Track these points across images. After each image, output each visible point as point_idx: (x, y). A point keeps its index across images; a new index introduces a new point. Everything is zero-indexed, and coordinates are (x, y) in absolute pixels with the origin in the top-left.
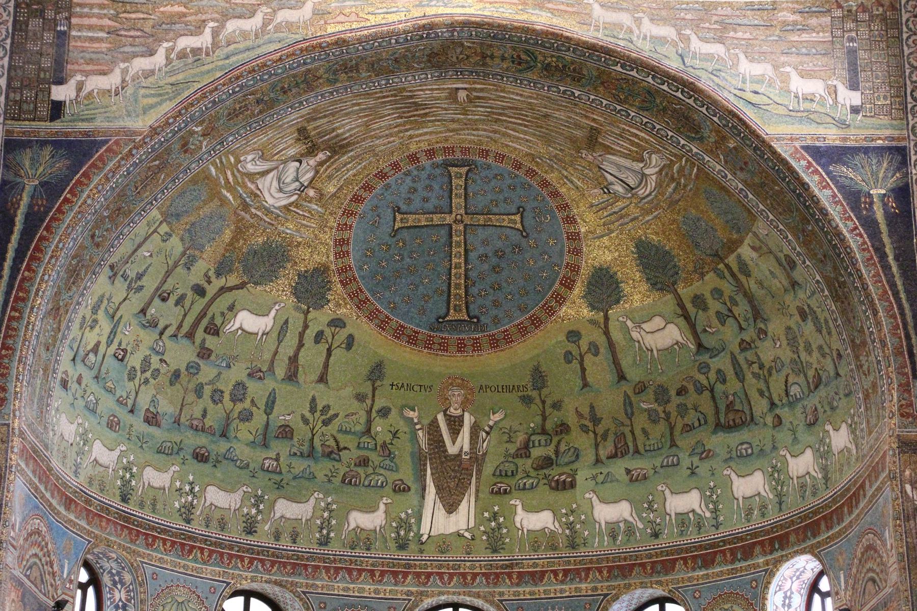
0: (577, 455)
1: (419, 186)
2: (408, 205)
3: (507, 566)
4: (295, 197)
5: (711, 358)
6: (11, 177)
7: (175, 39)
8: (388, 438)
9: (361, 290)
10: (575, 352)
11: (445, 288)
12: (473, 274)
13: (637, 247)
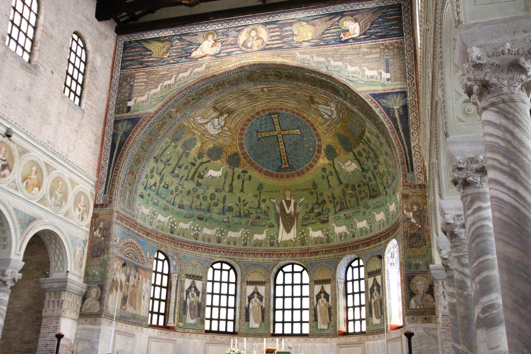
0: (329, 211)
1: (263, 122)
3: (307, 250)
6: (116, 132)
7: (163, 82)
8: (266, 209)
10: (325, 175)
12: (288, 151)
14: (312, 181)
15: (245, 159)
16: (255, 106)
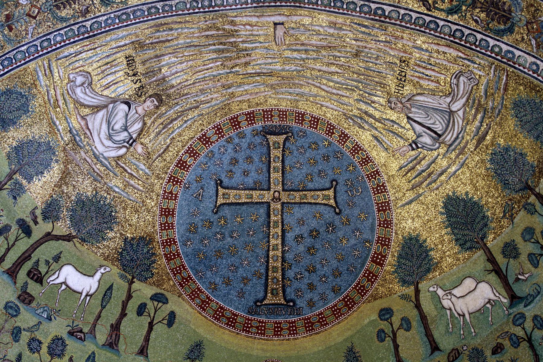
1: (241, 157)
2: (231, 178)
4: (124, 150)
5: (525, 306)
9: (184, 267)
10: (388, 330)
11: (263, 271)
12: (289, 256)
13: (445, 206)
14: (344, 349)
15: (169, 259)
16: (232, 95)
